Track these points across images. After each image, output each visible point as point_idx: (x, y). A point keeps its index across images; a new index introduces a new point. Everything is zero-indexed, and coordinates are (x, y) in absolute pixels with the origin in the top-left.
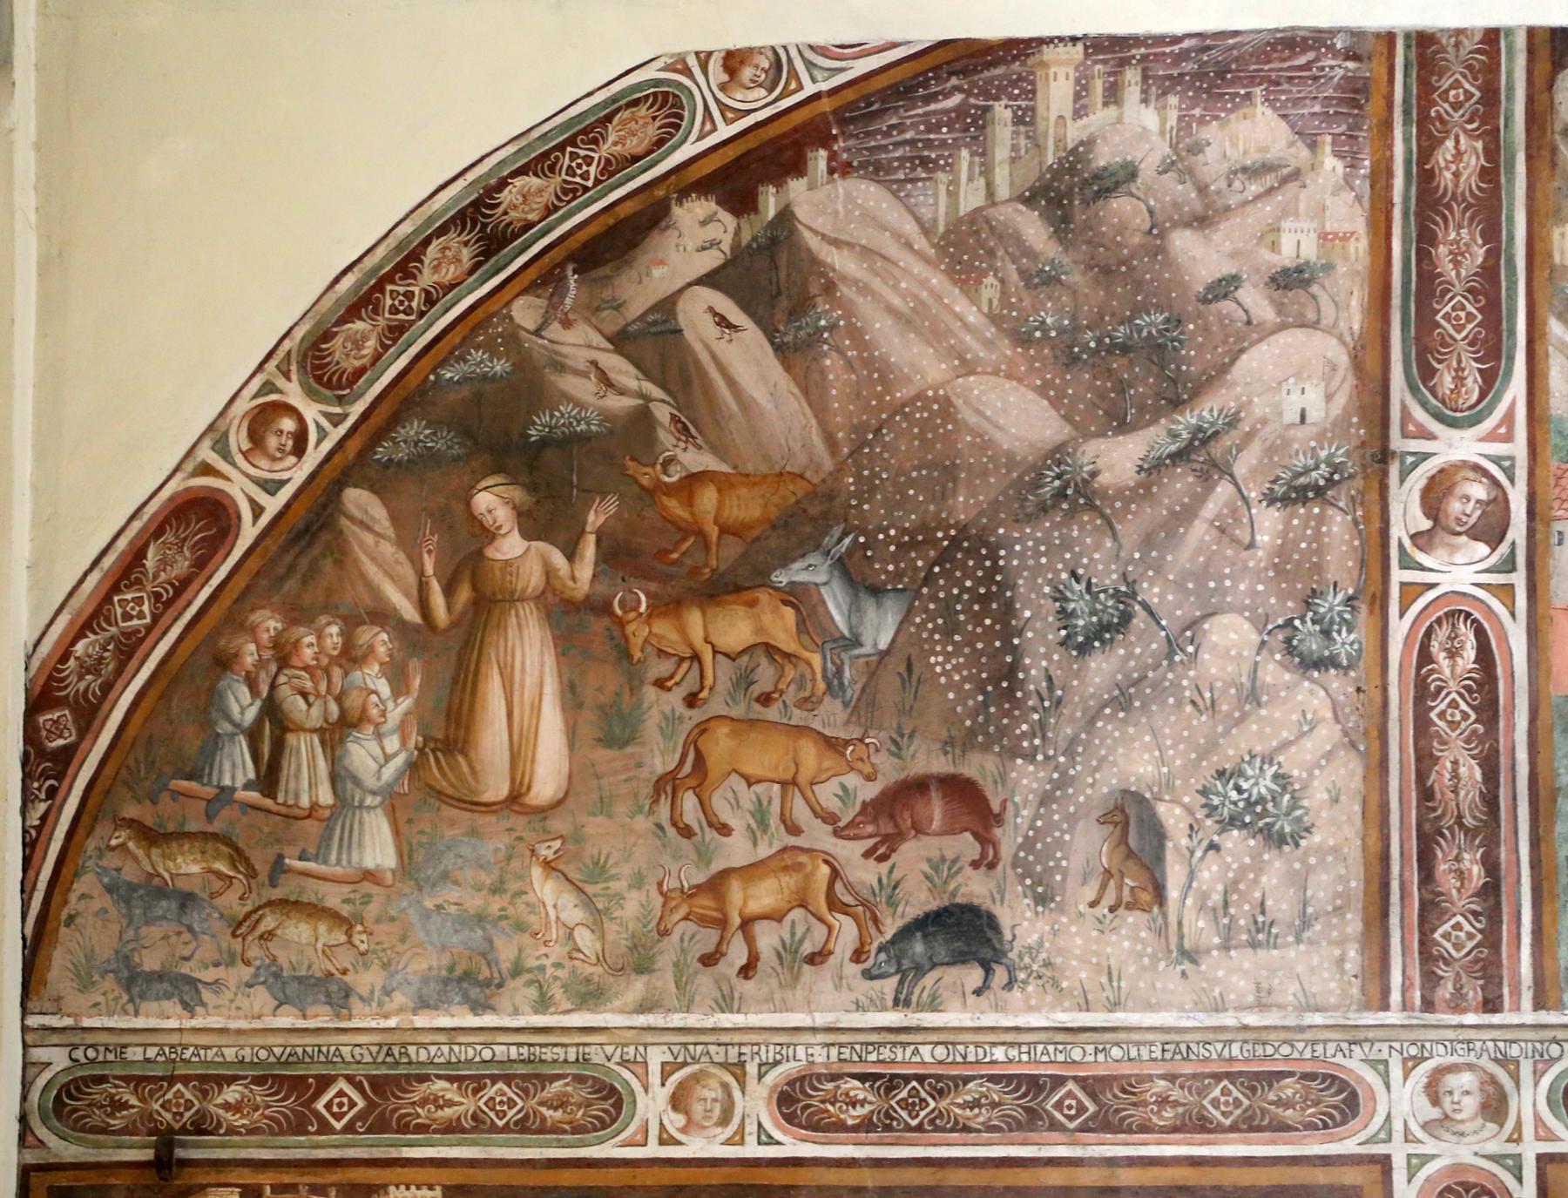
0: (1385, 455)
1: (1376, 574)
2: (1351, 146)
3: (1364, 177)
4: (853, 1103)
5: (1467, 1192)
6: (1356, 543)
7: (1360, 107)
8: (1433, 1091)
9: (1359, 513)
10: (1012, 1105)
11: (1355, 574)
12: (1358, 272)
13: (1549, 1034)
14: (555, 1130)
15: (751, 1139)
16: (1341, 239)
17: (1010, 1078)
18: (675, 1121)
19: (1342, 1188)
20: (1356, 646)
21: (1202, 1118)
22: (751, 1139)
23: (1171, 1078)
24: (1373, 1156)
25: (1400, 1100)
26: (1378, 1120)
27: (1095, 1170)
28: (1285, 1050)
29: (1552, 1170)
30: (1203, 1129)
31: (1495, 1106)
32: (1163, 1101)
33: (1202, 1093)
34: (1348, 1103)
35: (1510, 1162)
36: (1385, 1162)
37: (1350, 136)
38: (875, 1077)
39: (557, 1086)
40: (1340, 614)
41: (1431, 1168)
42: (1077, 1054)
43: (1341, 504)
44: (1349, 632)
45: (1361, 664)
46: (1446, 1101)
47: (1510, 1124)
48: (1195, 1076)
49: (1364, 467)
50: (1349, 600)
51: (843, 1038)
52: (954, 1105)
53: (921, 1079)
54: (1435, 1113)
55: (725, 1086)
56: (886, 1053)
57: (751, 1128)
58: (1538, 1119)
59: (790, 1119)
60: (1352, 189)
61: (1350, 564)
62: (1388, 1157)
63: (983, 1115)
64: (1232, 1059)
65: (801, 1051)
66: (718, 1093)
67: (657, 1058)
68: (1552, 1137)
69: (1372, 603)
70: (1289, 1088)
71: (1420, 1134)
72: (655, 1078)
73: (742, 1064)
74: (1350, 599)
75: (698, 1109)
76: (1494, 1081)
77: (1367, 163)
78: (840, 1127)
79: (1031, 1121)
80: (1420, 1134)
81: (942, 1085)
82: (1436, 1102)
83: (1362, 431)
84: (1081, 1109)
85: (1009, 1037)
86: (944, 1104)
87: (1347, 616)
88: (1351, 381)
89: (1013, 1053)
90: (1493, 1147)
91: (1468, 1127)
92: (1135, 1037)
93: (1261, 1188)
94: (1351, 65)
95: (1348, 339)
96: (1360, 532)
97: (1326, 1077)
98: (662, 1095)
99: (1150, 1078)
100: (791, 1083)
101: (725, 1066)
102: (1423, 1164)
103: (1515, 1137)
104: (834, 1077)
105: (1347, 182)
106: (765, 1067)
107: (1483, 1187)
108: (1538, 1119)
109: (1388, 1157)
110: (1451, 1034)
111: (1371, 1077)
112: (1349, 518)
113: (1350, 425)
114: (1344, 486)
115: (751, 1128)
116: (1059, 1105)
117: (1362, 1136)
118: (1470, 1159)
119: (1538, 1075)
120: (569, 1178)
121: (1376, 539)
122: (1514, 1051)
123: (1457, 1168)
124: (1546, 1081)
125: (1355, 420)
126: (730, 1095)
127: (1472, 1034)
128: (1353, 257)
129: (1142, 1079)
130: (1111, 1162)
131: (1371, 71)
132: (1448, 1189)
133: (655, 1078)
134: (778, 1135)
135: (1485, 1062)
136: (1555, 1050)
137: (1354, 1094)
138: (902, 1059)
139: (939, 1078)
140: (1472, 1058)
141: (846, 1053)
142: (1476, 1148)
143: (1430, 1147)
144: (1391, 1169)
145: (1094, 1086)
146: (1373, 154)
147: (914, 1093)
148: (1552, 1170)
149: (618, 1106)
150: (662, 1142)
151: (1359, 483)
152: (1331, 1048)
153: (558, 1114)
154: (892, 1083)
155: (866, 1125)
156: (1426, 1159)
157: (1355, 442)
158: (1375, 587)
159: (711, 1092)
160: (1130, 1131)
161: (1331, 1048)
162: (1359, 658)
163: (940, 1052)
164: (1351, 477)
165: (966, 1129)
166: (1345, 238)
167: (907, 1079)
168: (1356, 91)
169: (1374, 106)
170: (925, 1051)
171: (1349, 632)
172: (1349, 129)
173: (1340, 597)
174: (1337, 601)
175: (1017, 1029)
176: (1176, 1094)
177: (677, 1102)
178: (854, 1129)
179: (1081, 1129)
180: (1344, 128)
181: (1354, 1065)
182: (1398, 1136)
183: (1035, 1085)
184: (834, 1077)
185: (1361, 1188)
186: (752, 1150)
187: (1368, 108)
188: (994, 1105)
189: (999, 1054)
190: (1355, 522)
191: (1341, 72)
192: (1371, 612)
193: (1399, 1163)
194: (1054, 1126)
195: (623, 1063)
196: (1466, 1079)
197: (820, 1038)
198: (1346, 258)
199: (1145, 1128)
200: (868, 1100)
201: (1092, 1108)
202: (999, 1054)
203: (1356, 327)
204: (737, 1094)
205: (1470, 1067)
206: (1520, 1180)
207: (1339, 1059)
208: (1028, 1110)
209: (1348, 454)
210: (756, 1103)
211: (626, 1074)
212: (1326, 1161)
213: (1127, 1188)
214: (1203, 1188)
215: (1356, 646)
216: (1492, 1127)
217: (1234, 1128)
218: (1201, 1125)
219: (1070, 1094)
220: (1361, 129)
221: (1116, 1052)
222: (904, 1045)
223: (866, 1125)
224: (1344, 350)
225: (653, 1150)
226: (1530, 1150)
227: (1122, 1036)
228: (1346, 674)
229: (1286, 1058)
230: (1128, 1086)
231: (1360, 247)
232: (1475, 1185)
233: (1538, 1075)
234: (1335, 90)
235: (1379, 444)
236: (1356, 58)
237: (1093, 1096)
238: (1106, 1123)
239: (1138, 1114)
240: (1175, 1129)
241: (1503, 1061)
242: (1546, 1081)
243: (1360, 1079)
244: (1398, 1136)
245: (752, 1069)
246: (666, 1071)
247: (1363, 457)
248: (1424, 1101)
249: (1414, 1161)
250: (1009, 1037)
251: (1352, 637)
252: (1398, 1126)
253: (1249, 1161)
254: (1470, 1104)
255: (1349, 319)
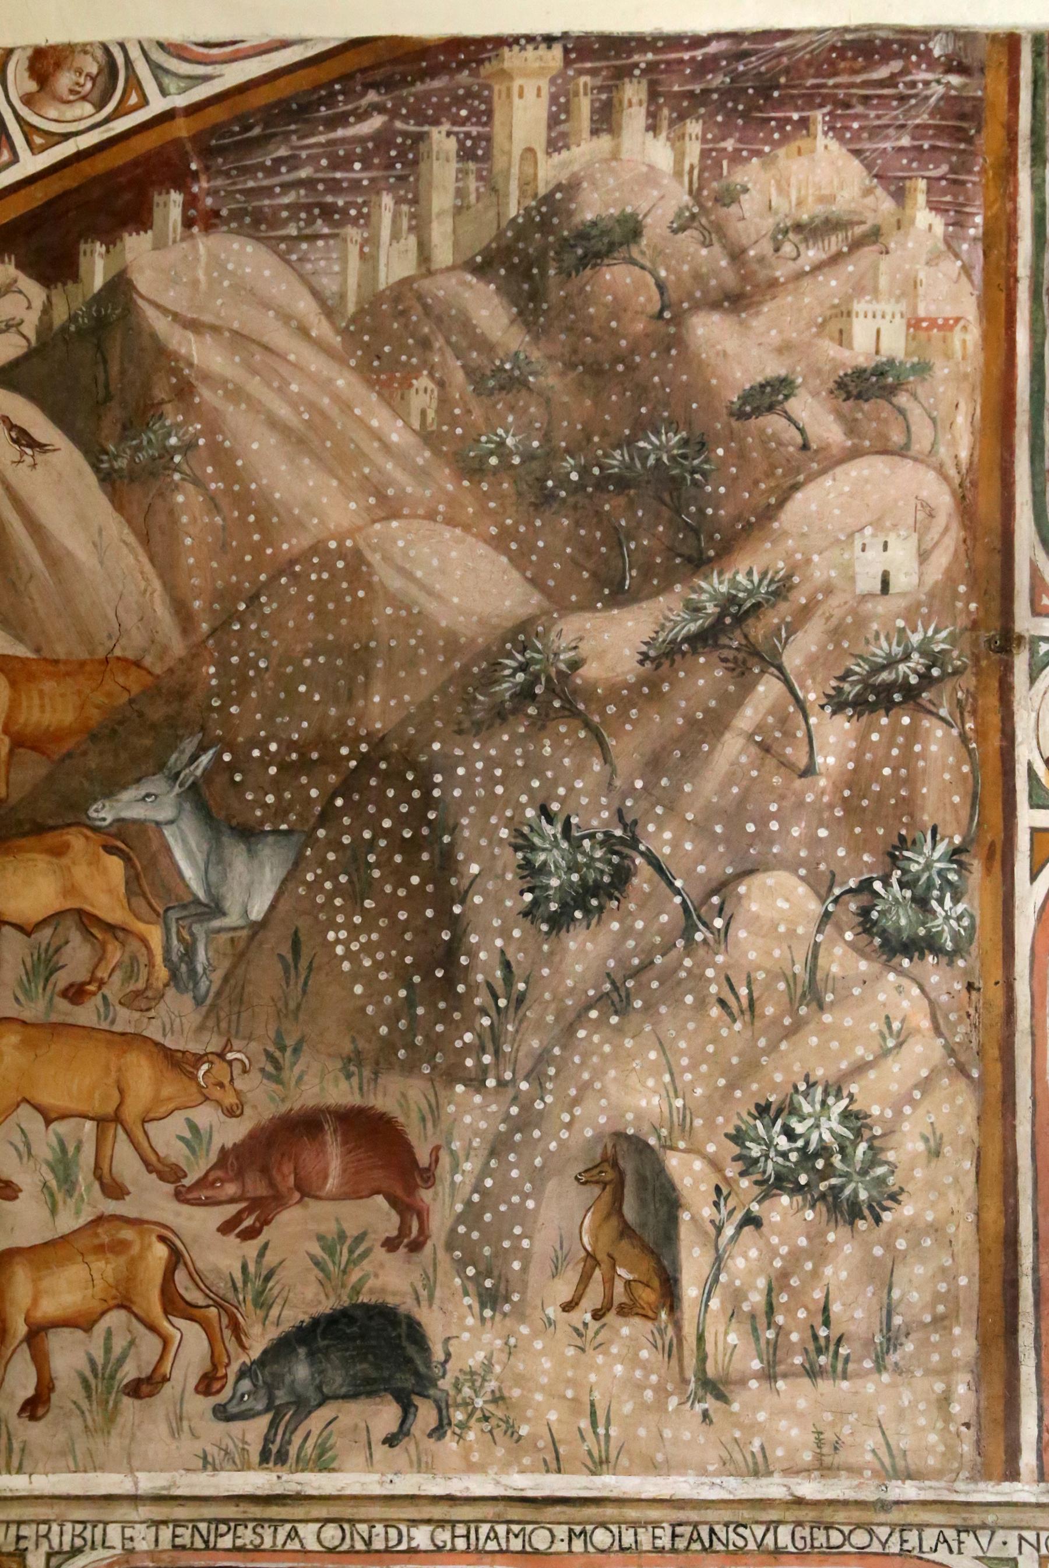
0: (1007, 641)
1: (995, 814)
2: (955, 196)
3: (975, 239)
6: (966, 769)
7: (969, 140)
9: (970, 725)
11: (964, 814)
12: (966, 376)
16: (940, 328)
20: (966, 922)
37: (955, 182)
40: (941, 873)
43: (943, 712)
44: (956, 900)
45: (974, 949)
49: (976, 659)
50: (955, 854)
60: (957, 256)
61: (956, 799)
69: (990, 857)
74: (957, 851)
77: (979, 220)
83: (973, 606)
87: (952, 877)
88: (956, 533)
94: (955, 80)
95: (952, 472)
96: (970, 752)
105: (949, 246)
112: (955, 732)
113: (956, 596)
114: (948, 686)
121: (994, 763)
125: (962, 589)
128: (959, 354)
131: (984, 89)
146: (987, 207)
151: (968, 680)
157: (963, 621)
158: (994, 834)
162: (970, 941)
164: (957, 672)
166: (947, 326)
168: (963, 117)
169: (989, 140)
171: (956, 900)
172: (953, 170)
173: (942, 848)
174: (936, 855)
180: (944, 168)
187: (980, 141)
190: (964, 738)
191: (940, 90)
192: (988, 870)
198: (948, 356)
203: (964, 454)
209: (952, 639)
215: (966, 922)
220: (970, 172)
224: (945, 488)
228: (951, 963)
231: (968, 339)
234: (932, 115)
235: (998, 624)
236: (962, 69)
247: (975, 643)
251: (960, 908)
255: (953, 443)
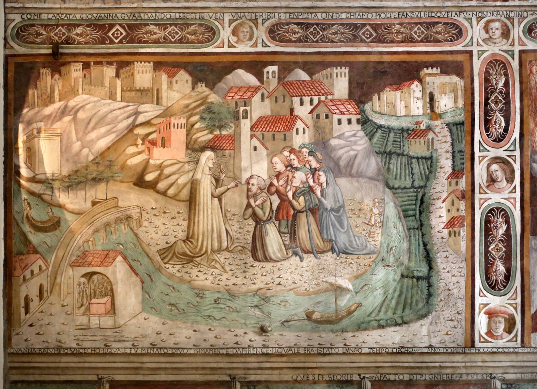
4: (295, 33)
5: (497, 63)
8: (486, 29)
10: (348, 34)
13: (523, 9)
14: (192, 42)
15: (260, 45)
17: (347, 24)
18: (233, 39)
19: (457, 62)
21: (411, 38)
22: (260, 45)
23: (401, 24)
24: (467, 51)
25: (475, 32)
26: (469, 38)
27: (376, 56)
28: (439, 14)
29: (523, 55)
30: (412, 42)
31: (506, 34)
32: (398, 32)
33: (411, 29)
34: (459, 33)
35: (510, 53)
36: (470, 53)
38: (302, 24)
39: (193, 27)
41: (485, 55)
42: (370, 16)
46: (491, 32)
47: (511, 40)
48: (409, 23)
51: (291, 11)
52: (328, 33)
53: (317, 24)
54: (487, 36)
55: (251, 27)
56: (306, 16)
57: (260, 41)
58: (520, 38)
59: (273, 38)
62: (471, 51)
63: (337, 37)
64: (421, 18)
65: (276, 15)
66: (248, 29)
67: (227, 17)
68: (524, 44)
70: (440, 28)
71: (482, 43)
72: (226, 25)
73: (256, 19)
75: (241, 35)
76: (506, 25)
78: (290, 41)
79: (355, 39)
80: (482, 43)
81: (324, 27)
82: (487, 32)
84: (371, 35)
85: (347, 10)
86: (325, 33)
89: (349, 15)
90: (505, 48)
91: (497, 41)
92: (389, 10)
93: (430, 62)
97: (452, 24)
98: (229, 30)
99: (394, 24)
100: (273, 26)
101: (250, 20)
102: (483, 54)
103: (512, 45)
104: (288, 24)
106: (264, 21)
107: (502, 61)
108: (520, 38)
109: (471, 51)
110: (492, 9)
111: (466, 24)
115: (260, 41)
116: (364, 34)
117: (463, 44)
118: (497, 52)
119: (520, 23)
120: (197, 59)
122: (513, 15)
123: (494, 55)
124: (522, 25)
126: (252, 30)
127: (499, 9)
129: (391, 25)
130: (381, 53)
132: (491, 62)
133: (226, 25)
134: (269, 44)
135: (503, 18)
136: (525, 14)
137: (461, 30)
138: (311, 18)
139: (323, 24)
140: (499, 17)
141: (292, 15)
142: (500, 48)
143: (485, 47)
144: (472, 55)
145: (375, 27)
147: (315, 29)
148: (523, 55)
149: (214, 34)
150: (229, 47)
152: (454, 14)
153: (193, 37)
154: (307, 26)
155: (299, 41)
156: (484, 52)
159: (246, 29)
160: (387, 42)
161: (454, 14)
163: (324, 15)
165: (333, 42)
167: (313, 24)
170: (319, 15)
175: (350, 7)
176: (403, 30)
177: (234, 33)
178: (295, 42)
179: (372, 42)
181: (461, 20)
182: (475, 44)
183: (356, 27)
184: (288, 24)
185: (463, 61)
186: (260, 49)
188: (342, 33)
189: (344, 16)
193: (475, 53)
194: (362, 41)
195: (216, 19)
196: (497, 24)
197: (283, 10)
199: (392, 42)
200: (300, 32)
201: (375, 35)
202: (344, 16)
204: (255, 30)
205: (498, 20)
206: (513, 59)
207: (456, 18)
208: (353, 35)
210: (261, 33)
211: (217, 23)
212: (451, 52)
213: (387, 62)
214: (412, 62)
216: (505, 41)
217: (422, 41)
218: (410, 40)
219: (367, 30)
221: (383, 15)
222: (312, 13)
223: (299, 41)
225: (226, 49)
226: (517, 49)
227: (385, 10)
229: (439, 17)
230: (387, 27)
232: (499, 61)
233: (520, 23)
237: (375, 31)
238: (380, 40)
239: (390, 37)
240: (402, 42)
241: (509, 18)
242: (522, 25)
243: (463, 25)
244: (475, 44)
245: (260, 21)
246: (231, 22)
248: (483, 32)
249: (480, 52)
250: (347, 10)
252: (475, 40)
253: (426, 53)
254: (498, 33)
